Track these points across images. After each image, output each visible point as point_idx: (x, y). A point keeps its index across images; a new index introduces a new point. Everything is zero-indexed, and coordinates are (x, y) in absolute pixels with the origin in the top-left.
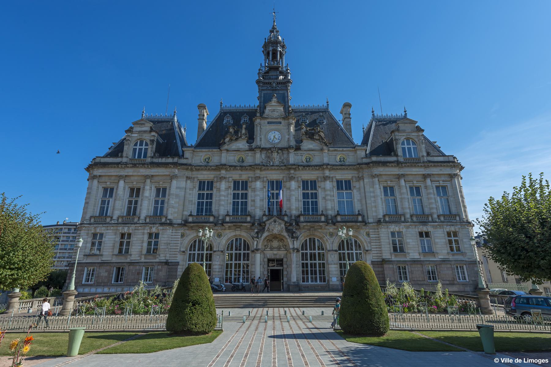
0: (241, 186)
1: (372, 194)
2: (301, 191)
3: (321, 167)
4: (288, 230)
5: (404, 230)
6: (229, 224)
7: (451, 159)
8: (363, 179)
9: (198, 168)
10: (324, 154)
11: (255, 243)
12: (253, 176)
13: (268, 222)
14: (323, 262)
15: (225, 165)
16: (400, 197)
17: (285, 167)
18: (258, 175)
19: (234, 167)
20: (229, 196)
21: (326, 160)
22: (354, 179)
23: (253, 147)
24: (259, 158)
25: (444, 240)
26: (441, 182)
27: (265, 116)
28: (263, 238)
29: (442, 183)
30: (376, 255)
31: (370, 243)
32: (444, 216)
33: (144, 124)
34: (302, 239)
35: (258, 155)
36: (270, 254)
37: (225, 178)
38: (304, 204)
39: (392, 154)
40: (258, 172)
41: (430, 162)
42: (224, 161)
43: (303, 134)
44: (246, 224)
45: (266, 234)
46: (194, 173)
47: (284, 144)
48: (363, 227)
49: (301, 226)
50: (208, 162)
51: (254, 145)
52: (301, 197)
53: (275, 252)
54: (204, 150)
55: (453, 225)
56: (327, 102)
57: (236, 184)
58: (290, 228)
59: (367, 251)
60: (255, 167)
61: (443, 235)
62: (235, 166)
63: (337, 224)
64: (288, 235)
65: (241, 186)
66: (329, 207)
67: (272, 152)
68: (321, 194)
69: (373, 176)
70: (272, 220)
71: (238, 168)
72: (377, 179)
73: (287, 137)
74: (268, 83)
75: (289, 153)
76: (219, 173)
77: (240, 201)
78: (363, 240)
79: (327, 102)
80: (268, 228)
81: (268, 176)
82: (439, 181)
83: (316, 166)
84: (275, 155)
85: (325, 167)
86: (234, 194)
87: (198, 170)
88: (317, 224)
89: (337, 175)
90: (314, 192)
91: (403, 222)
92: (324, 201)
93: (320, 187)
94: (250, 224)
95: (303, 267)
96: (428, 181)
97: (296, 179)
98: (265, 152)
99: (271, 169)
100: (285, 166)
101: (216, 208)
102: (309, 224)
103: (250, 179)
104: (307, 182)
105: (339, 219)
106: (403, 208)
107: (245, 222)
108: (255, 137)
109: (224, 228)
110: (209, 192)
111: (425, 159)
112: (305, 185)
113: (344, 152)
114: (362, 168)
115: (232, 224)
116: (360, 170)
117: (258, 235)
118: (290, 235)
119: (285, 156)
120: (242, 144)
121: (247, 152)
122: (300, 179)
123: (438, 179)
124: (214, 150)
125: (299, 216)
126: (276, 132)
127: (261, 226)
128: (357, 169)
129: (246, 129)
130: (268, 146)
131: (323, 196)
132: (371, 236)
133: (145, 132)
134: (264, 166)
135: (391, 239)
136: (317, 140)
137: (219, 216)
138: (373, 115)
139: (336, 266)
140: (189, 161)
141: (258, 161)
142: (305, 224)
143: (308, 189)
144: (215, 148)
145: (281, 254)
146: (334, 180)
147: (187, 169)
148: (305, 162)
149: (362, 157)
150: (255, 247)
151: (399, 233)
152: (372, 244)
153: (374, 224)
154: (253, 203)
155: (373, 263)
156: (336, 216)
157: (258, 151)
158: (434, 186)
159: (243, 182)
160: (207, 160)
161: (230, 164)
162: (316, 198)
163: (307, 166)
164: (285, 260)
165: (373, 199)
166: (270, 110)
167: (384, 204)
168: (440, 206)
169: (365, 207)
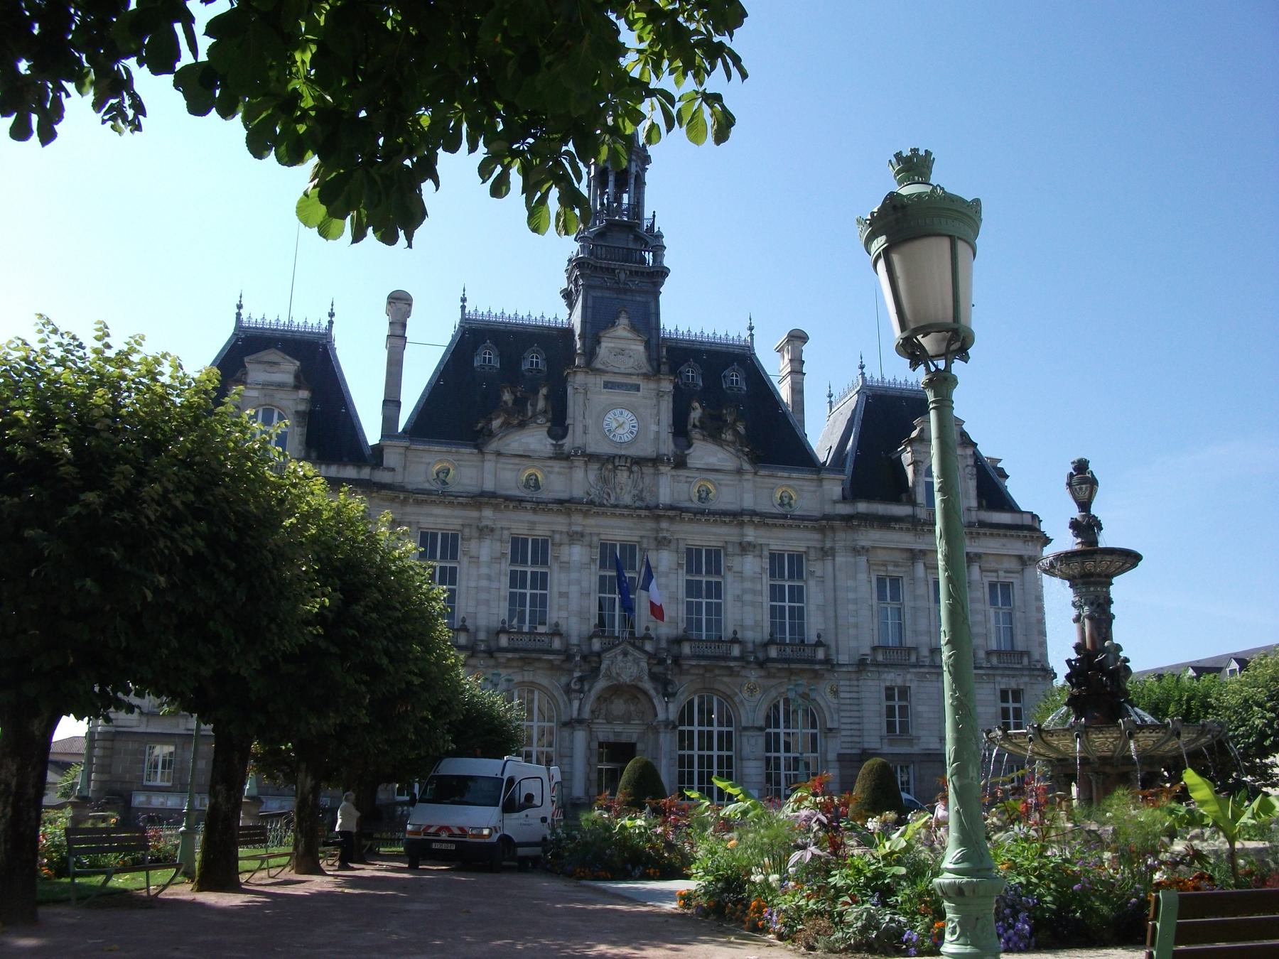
0: (530, 554)
1: (851, 595)
2: (682, 577)
3: (736, 517)
4: (654, 677)
5: (913, 685)
6: (510, 655)
7: (1027, 520)
8: (834, 557)
9: (421, 497)
10: (745, 484)
11: (576, 704)
12: (564, 529)
13: (608, 655)
14: (729, 753)
15: (493, 495)
16: (912, 604)
17: (647, 513)
18: (578, 529)
19: (518, 502)
20: (503, 578)
21: (748, 502)
22: (812, 555)
23: (566, 448)
24: (580, 481)
25: (993, 710)
26: (1001, 574)
27: (598, 364)
28: (593, 692)
29: (1003, 577)
30: (849, 739)
31: (839, 711)
32: (999, 653)
33: (275, 363)
34: (682, 698)
35: (579, 474)
36: (604, 732)
37: (492, 530)
38: (689, 610)
39: (904, 497)
40: (578, 519)
41: (982, 524)
42: (489, 486)
43: (695, 426)
44: (551, 657)
45: (601, 684)
46: (409, 509)
47: (648, 450)
48: (827, 675)
49: (685, 667)
50: (444, 483)
51: (568, 443)
52: (682, 592)
53: (618, 729)
54: (437, 448)
55: (1014, 676)
56: (751, 329)
57: (518, 545)
58: (656, 669)
59: (830, 730)
60: (573, 507)
61: (992, 698)
62: (521, 501)
63: (770, 665)
64: (655, 689)
65: (530, 554)
66: (749, 621)
67: (616, 468)
68: (731, 587)
69: (857, 551)
70: (618, 650)
71: (529, 506)
72: (864, 559)
73: (654, 428)
74: (607, 269)
75: (657, 473)
76: (475, 514)
77: (528, 592)
78: (822, 704)
79: (751, 329)
80: (608, 669)
81: (601, 530)
82: (996, 571)
83: (724, 513)
84: (623, 476)
85: (746, 519)
86: (513, 573)
87: (419, 503)
88: (723, 664)
89: (771, 542)
90: (714, 579)
91: (915, 666)
92: (739, 604)
93: (729, 568)
94: (561, 657)
95: (681, 765)
96: (975, 569)
97: (673, 546)
98: (596, 466)
99: (614, 515)
100: (647, 508)
101: (471, 610)
102: (703, 663)
103: (557, 537)
104: (699, 552)
105: (773, 652)
106: (915, 632)
107: (549, 651)
108: (569, 421)
109: (491, 662)
110: (448, 565)
111: (974, 516)
112: (693, 559)
113: (791, 483)
114: (832, 528)
115: (517, 656)
116: (829, 534)
117: (583, 685)
118: (660, 688)
119: (647, 480)
120: (535, 439)
121: (550, 463)
122: (682, 546)
123: (993, 565)
124: (463, 450)
125: (678, 641)
126: (626, 413)
127: (591, 664)
128: (822, 530)
129: (546, 397)
130: (606, 449)
131: (739, 593)
132: (842, 695)
133: (281, 386)
134: (591, 503)
135: (885, 703)
136: (728, 443)
137: (477, 630)
138: (863, 374)
139: (758, 764)
140: (398, 478)
141: (578, 492)
142: (694, 663)
143: (699, 572)
144: (466, 446)
145: (630, 732)
146: (766, 553)
147: (393, 500)
148: (695, 499)
149: (835, 498)
150: (575, 715)
151: (904, 692)
152: (843, 714)
153: (850, 669)
154: (563, 601)
155: (841, 758)
156: (765, 645)
157: (579, 463)
158: (986, 581)
159: (535, 542)
160: (441, 475)
161: (503, 493)
162: (719, 596)
163: (703, 514)
164: (639, 746)
165: (851, 607)
166: (610, 350)
167: (875, 620)
168: (993, 630)
169: (832, 626)
